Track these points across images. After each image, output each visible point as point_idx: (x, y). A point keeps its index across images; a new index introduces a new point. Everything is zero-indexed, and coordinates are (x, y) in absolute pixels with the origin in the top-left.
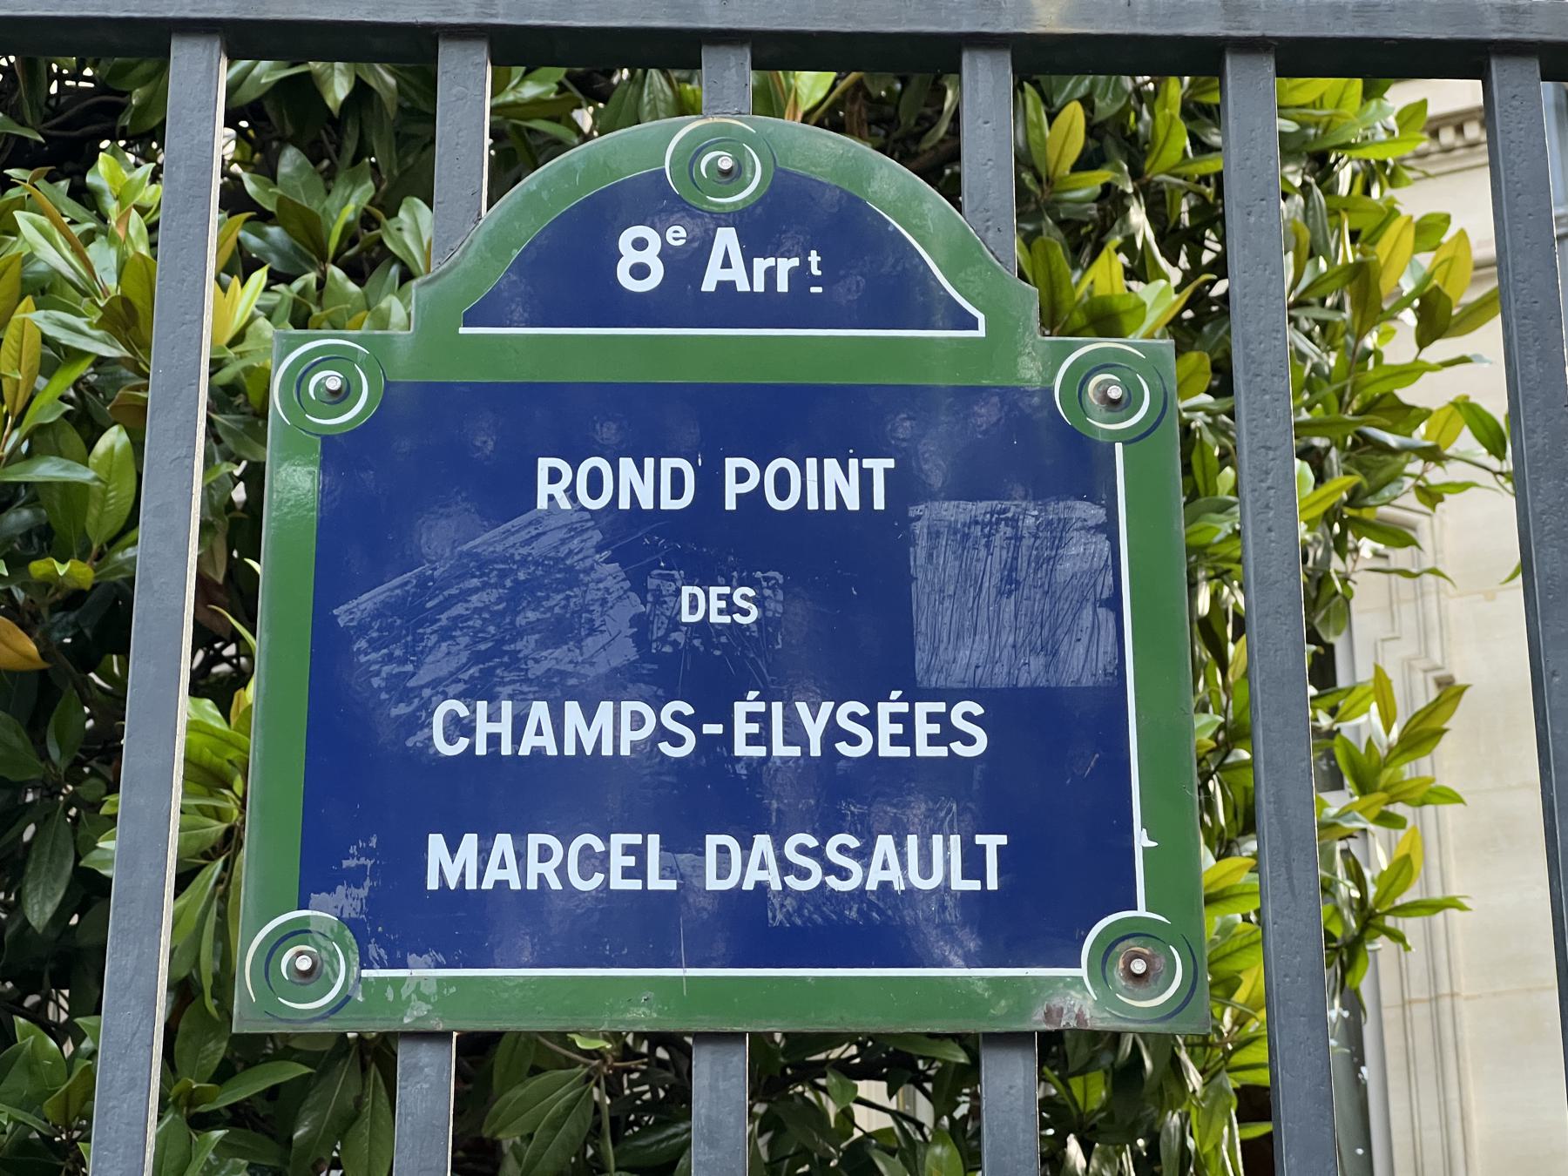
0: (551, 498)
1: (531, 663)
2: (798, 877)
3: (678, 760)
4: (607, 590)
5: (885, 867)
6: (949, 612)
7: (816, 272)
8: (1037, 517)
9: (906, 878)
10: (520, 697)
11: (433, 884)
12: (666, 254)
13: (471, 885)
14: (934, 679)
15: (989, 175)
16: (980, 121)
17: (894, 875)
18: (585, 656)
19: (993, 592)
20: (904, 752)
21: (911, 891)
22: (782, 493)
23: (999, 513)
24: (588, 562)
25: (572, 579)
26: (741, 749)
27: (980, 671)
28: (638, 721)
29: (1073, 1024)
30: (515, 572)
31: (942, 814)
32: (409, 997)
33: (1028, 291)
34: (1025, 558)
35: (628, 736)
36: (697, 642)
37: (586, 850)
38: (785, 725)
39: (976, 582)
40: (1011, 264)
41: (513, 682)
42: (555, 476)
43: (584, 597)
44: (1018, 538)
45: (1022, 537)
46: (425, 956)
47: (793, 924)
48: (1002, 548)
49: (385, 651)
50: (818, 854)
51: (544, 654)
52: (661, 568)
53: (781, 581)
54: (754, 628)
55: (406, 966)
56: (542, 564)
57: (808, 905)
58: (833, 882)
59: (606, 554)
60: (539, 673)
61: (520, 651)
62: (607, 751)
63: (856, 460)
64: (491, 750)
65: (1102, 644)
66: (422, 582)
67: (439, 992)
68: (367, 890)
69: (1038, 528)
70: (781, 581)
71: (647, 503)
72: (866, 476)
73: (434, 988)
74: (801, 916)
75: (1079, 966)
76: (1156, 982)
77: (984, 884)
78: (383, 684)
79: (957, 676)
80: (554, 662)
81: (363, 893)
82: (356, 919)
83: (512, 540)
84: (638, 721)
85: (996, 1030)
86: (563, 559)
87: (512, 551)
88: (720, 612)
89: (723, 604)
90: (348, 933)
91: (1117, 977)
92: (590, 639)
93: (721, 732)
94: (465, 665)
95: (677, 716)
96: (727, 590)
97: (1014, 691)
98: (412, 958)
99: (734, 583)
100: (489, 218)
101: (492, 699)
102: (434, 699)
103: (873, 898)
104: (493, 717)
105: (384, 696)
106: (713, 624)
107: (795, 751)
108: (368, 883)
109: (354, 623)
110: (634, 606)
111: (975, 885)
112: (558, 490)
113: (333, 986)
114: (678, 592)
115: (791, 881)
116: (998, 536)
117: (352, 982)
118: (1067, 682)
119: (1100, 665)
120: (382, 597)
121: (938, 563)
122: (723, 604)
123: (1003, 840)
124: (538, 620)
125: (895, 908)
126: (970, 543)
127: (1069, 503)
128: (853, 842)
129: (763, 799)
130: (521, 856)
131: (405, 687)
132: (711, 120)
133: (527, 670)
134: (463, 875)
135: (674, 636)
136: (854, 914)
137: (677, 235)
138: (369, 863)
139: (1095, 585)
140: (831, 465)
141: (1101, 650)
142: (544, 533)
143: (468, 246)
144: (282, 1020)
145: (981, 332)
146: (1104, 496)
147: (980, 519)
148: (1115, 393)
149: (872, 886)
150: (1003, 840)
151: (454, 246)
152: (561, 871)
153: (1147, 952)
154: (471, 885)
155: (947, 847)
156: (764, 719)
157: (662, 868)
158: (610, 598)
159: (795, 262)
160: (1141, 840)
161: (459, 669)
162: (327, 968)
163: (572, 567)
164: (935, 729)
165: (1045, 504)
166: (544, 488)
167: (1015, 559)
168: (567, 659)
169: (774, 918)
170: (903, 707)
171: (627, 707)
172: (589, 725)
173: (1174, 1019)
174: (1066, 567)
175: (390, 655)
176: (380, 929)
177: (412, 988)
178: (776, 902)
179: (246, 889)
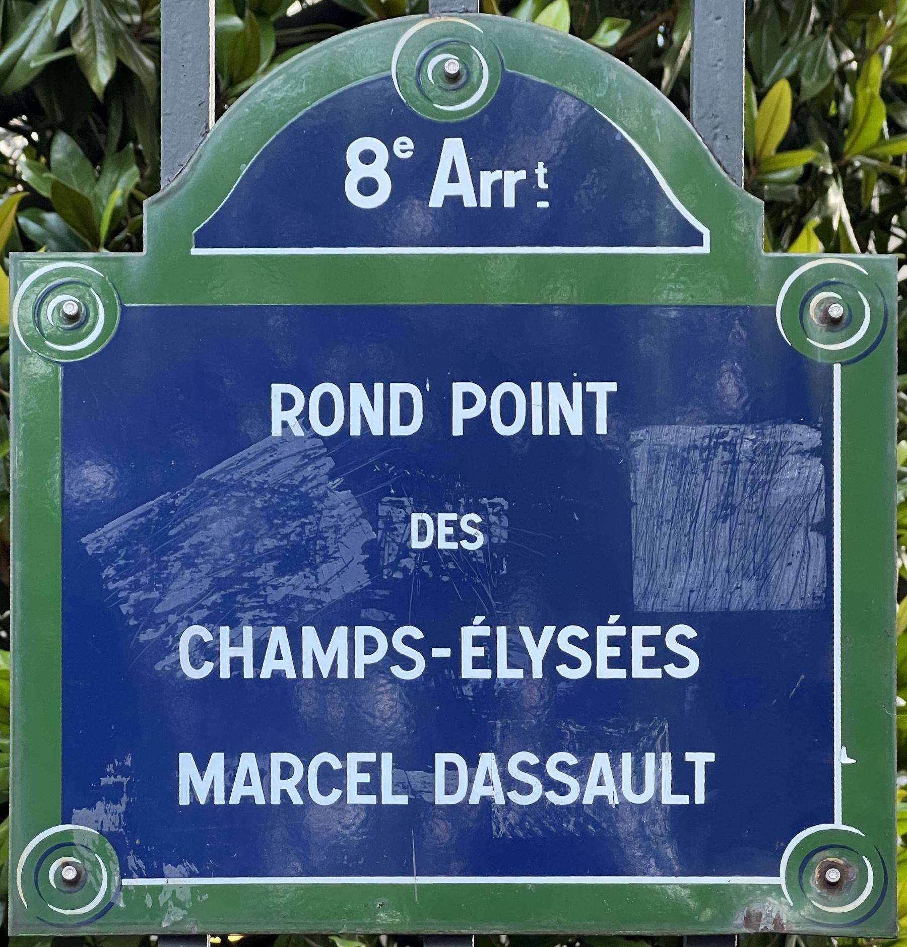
0: (285, 424)
1: (269, 589)
2: (520, 793)
3: (409, 682)
4: (340, 517)
5: (601, 783)
6: (667, 537)
7: (543, 185)
8: (754, 442)
9: (620, 793)
10: (260, 622)
11: (184, 800)
12: (394, 167)
13: (219, 800)
14: (650, 603)
15: (719, 77)
16: (711, 17)
17: (609, 791)
18: (321, 582)
19: (710, 517)
20: (621, 674)
21: (624, 803)
22: (508, 417)
23: (718, 437)
24: (322, 489)
25: (306, 507)
26: (468, 671)
27: (694, 595)
28: (371, 645)
29: (771, 928)
30: (252, 500)
31: (656, 733)
32: (166, 903)
33: (754, 203)
34: (741, 483)
35: (362, 660)
36: (426, 569)
37: (325, 768)
38: (509, 648)
39: (693, 507)
40: (737, 174)
41: (253, 608)
42: (288, 402)
43: (317, 524)
44: (735, 462)
45: (739, 462)
46: (180, 866)
47: (515, 836)
48: (719, 472)
49: (131, 578)
50: (539, 770)
51: (282, 580)
52: (390, 495)
53: (506, 508)
54: (480, 554)
55: (162, 876)
56: (277, 492)
57: (529, 818)
58: (553, 797)
59: (339, 481)
60: (277, 599)
61: (259, 578)
62: (342, 674)
63: (580, 384)
64: (236, 673)
65: (811, 568)
66: (165, 509)
67: (193, 899)
68: (124, 806)
69: (754, 451)
70: (506, 508)
71: (377, 429)
72: (589, 400)
73: (188, 896)
74: (523, 828)
75: (778, 875)
76: (849, 889)
77: (692, 798)
78: (132, 611)
79: (673, 600)
80: (291, 588)
81: (121, 808)
82: (116, 832)
83: (248, 467)
84: (371, 645)
85: (701, 933)
86: (297, 487)
87: (248, 478)
88: (448, 538)
89: (450, 531)
90: (108, 845)
91: (812, 885)
92: (324, 565)
93: (449, 655)
94: (207, 591)
95: (408, 641)
96: (453, 517)
97: (725, 615)
98: (167, 868)
99: (462, 510)
100: (217, 130)
101: (234, 624)
102: (179, 624)
103: (589, 812)
104: (235, 642)
105: (132, 622)
106: (441, 550)
107: (518, 674)
108: (124, 799)
109: (101, 552)
110: (367, 533)
111: (684, 800)
112: (291, 416)
113: (96, 893)
114: (408, 519)
115: (514, 796)
116: (716, 460)
117: (114, 890)
118: (777, 607)
119: (809, 588)
120: (127, 526)
121: (657, 489)
122: (450, 531)
123: (711, 757)
124: (276, 547)
125: (609, 821)
126: (688, 468)
127: (786, 426)
128: (571, 759)
129: (488, 719)
130: (265, 774)
131: (152, 613)
132: (437, 19)
133: (266, 596)
134: (212, 791)
135: (404, 562)
136: (571, 827)
137: (404, 146)
138: (125, 781)
139: (807, 509)
140: (556, 388)
141: (811, 575)
142: (278, 461)
143: (197, 161)
144: (52, 925)
145: (705, 249)
146: (821, 419)
147: (698, 443)
148: (836, 311)
149: (588, 800)
150: (711, 757)
151: (183, 161)
152: (303, 788)
153: (841, 862)
154: (219, 800)
155: (658, 763)
156: (489, 643)
157: (395, 784)
158: (343, 525)
159: (522, 175)
160: (841, 757)
161: (202, 596)
162: (90, 878)
163: (306, 494)
164: (651, 651)
165: (763, 428)
166: (278, 415)
167: (731, 484)
168: (303, 586)
169: (498, 829)
170: (621, 631)
171: (361, 632)
172: (325, 650)
173: (863, 924)
174: (781, 491)
175: (136, 582)
176: (138, 841)
177: (169, 895)
178: (500, 816)
179: (13, 805)
